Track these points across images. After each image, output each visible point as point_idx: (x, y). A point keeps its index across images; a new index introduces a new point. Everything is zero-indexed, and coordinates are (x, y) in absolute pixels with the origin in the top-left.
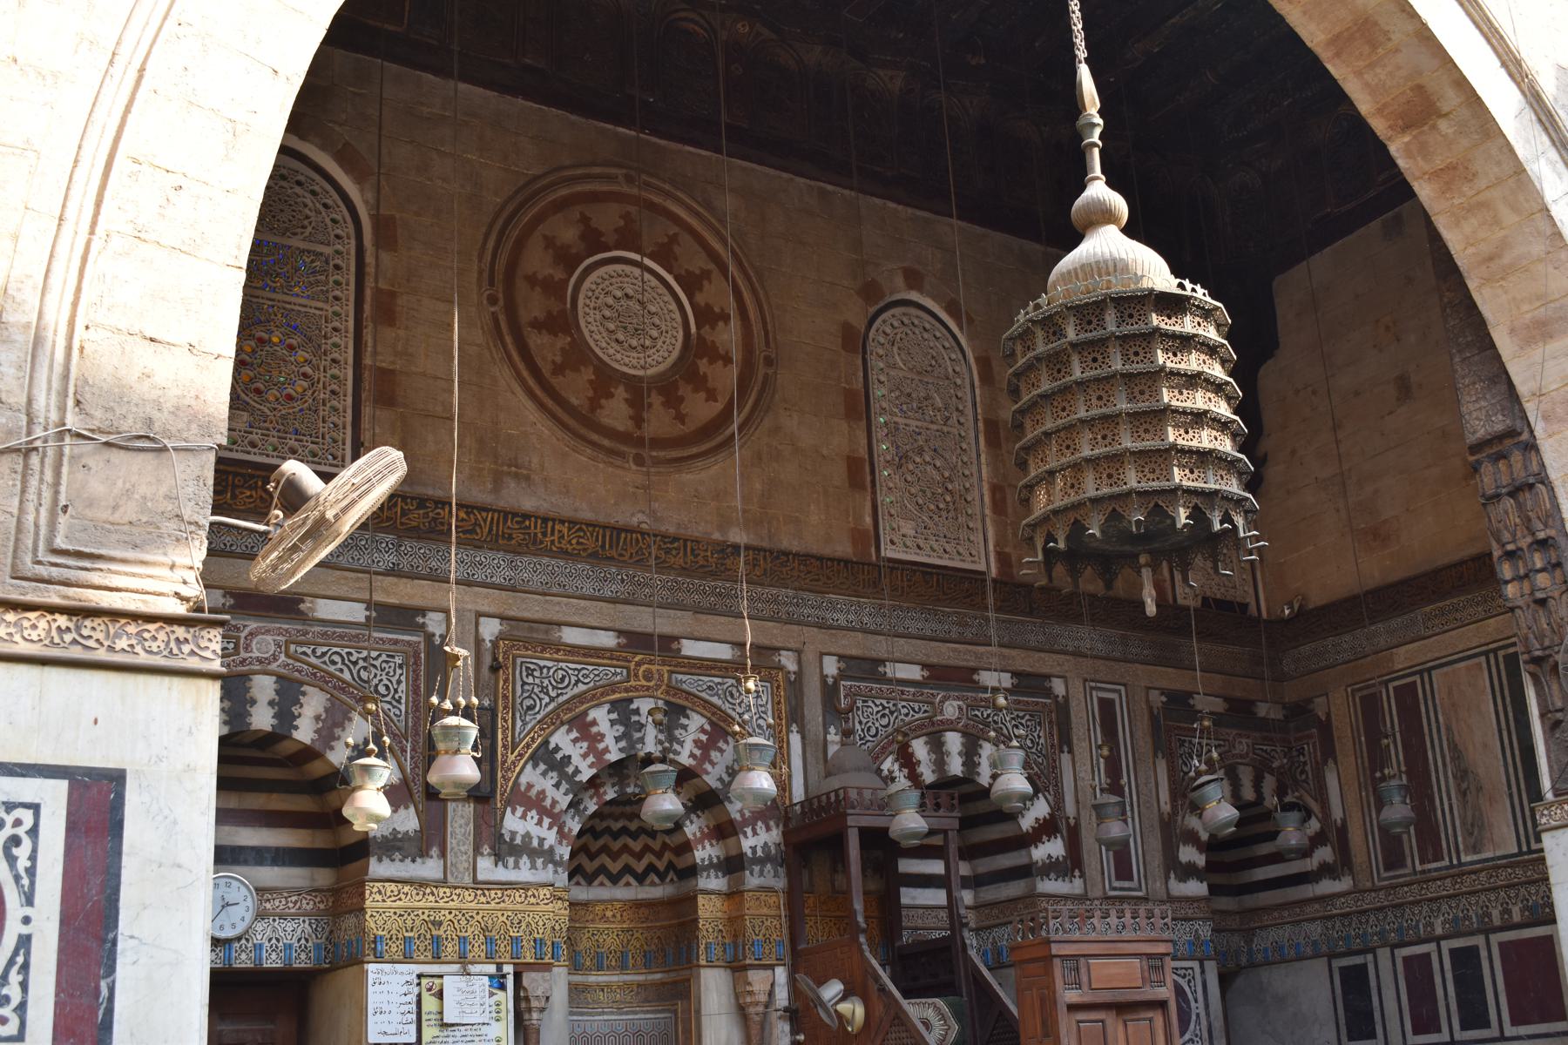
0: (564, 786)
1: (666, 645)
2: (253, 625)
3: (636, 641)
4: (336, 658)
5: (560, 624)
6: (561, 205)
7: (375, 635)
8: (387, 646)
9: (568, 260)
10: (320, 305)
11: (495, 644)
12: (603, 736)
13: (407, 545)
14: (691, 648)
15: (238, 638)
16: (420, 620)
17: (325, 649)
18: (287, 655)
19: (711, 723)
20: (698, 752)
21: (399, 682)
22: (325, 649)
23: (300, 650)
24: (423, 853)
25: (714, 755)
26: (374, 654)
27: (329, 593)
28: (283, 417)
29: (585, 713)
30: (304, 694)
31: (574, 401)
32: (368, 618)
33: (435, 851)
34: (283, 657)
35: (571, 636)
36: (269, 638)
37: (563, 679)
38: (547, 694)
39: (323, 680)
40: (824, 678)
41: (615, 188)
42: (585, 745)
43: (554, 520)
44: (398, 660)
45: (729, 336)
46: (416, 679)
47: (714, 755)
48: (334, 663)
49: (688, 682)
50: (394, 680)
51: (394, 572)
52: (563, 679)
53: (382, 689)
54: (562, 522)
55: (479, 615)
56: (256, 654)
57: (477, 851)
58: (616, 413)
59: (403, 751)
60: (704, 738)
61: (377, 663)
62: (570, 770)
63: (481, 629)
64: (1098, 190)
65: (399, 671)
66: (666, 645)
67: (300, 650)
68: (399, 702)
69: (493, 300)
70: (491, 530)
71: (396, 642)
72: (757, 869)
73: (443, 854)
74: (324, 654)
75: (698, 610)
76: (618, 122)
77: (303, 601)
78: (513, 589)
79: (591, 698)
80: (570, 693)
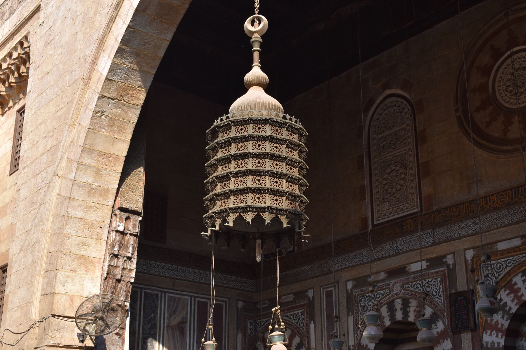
0: (506, 317)
2: (393, 281)
4: (418, 286)
7: (430, 272)
8: (435, 275)
9: (486, 71)
10: (404, 149)
11: (472, 260)
12: (520, 289)
15: (389, 288)
16: (445, 260)
17: (414, 283)
18: (404, 290)
21: (440, 288)
22: (414, 283)
23: (407, 286)
26: (430, 280)
27: (414, 261)
28: (398, 198)
29: (511, 280)
30: (410, 303)
31: (497, 135)
32: (427, 266)
34: (402, 291)
35: (502, 246)
36: (398, 285)
37: (500, 268)
38: (494, 276)
39: (414, 296)
40: (347, 291)
42: (512, 295)
43: (489, 196)
44: (439, 280)
46: (446, 285)
48: (418, 288)
50: (438, 288)
51: (434, 244)
52: (500, 266)
53: (434, 293)
54: (493, 195)
55: (465, 250)
56: (395, 292)
58: (516, 130)
59: (444, 316)
61: (431, 283)
62: (507, 309)
63: (466, 256)
64: (256, 72)
65: (439, 284)
67: (407, 286)
68: (441, 296)
69: (457, 111)
70: (465, 212)
71: (437, 272)
74: (414, 285)
77: (406, 267)
79: (512, 273)
80: (504, 273)
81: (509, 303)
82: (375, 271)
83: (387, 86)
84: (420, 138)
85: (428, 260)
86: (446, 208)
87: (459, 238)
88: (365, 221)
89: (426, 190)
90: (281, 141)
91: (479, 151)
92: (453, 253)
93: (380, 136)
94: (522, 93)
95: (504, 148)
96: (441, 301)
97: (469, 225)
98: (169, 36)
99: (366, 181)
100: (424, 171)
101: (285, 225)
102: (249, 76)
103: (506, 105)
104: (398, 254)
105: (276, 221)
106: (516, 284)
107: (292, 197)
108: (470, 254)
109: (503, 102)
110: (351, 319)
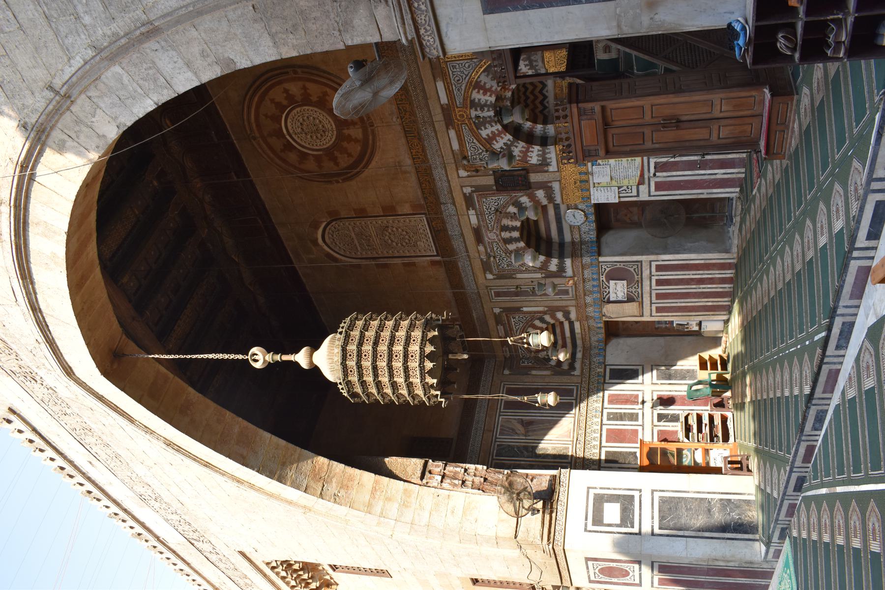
1: (447, 111)
2: (486, 239)
3: (449, 122)
5: (453, 151)
6: (284, 161)
9: (303, 156)
11: (468, 171)
13: (443, 200)
14: (444, 99)
19: (474, 89)
20: (489, 94)
24: (551, 187)
25: (488, 86)
31: (359, 148)
33: (550, 185)
35: (456, 146)
39: (499, 221)
40: (494, 279)
41: (261, 142)
45: (294, 88)
47: (488, 86)
49: (459, 100)
51: (454, 204)
55: (459, 177)
57: (547, 171)
60: (481, 92)
64: (301, 358)
66: (447, 111)
69: (338, 182)
72: (534, 64)
73: (550, 182)
75: (426, 98)
76: (233, 144)
78: (445, 167)
80: (478, 145)
81: (505, 141)
82: (477, 255)
83: (315, 242)
84: (362, 213)
85: (468, 209)
86: (423, 193)
87: (449, 182)
88: (433, 263)
89: (407, 209)
90: (362, 336)
91: (373, 164)
92: (462, 187)
93: (359, 249)
94: (323, 126)
95: (371, 142)
96: (503, 198)
97: (438, 173)
98: (267, 435)
99: (399, 261)
100: (390, 210)
101: (436, 333)
102: (304, 364)
103: (333, 140)
104: (462, 234)
105: (432, 341)
106: (488, 135)
107: (412, 327)
108: (463, 173)
109: (331, 143)
110: (519, 276)
